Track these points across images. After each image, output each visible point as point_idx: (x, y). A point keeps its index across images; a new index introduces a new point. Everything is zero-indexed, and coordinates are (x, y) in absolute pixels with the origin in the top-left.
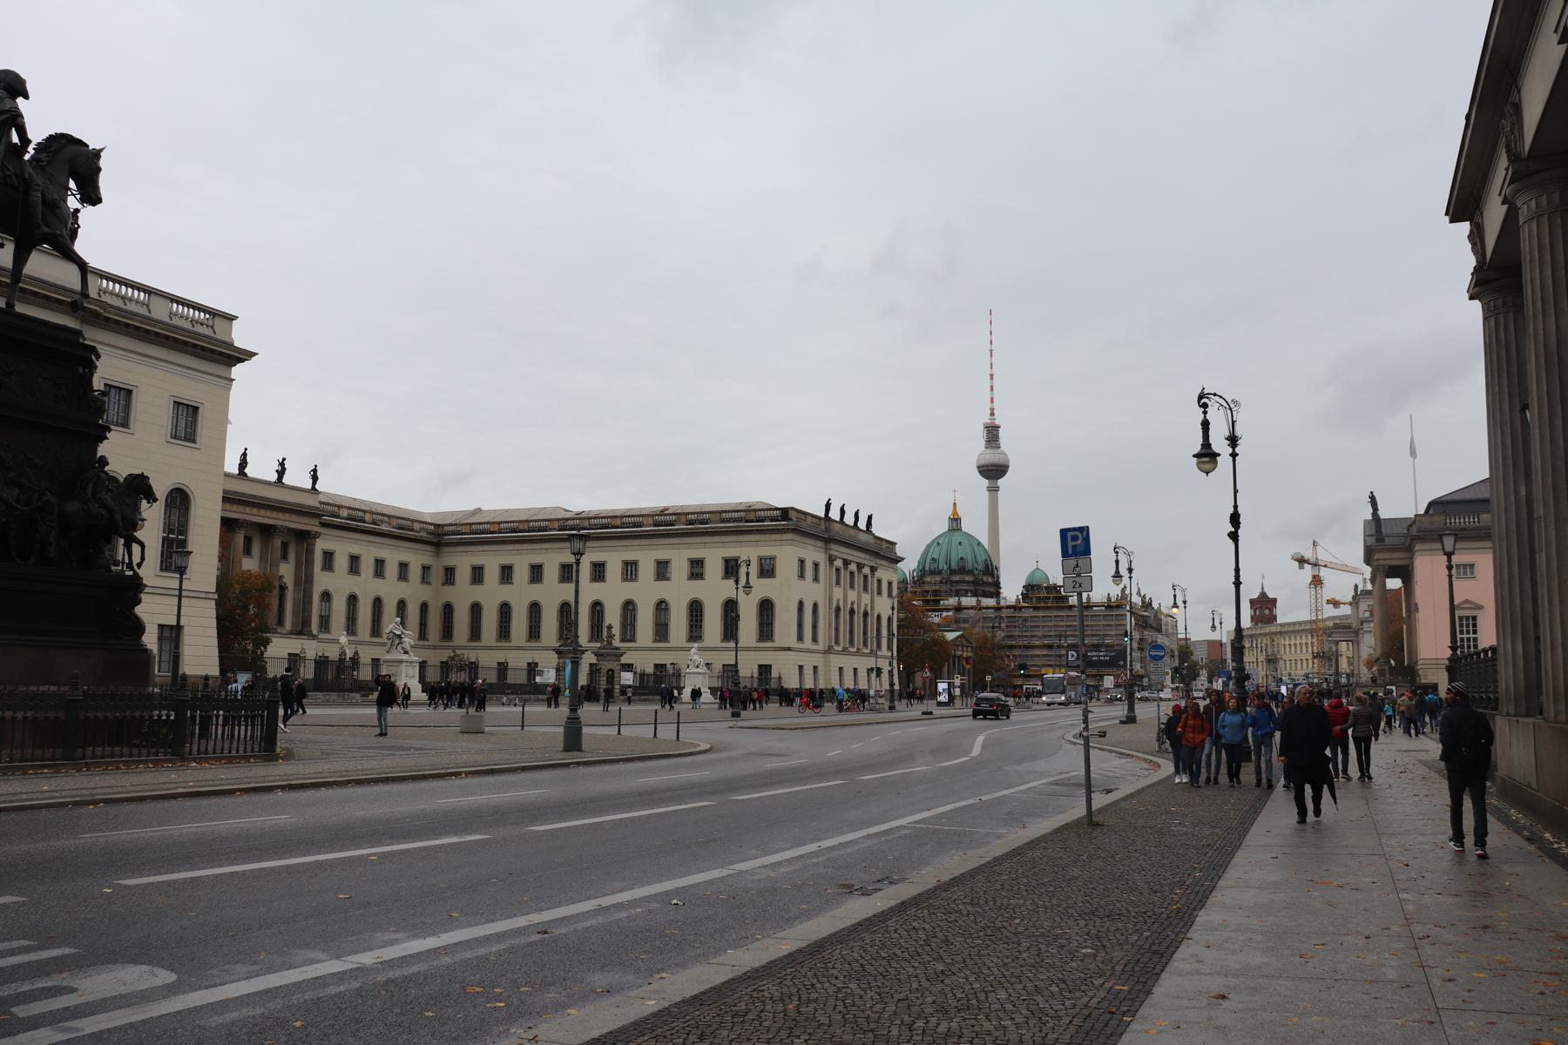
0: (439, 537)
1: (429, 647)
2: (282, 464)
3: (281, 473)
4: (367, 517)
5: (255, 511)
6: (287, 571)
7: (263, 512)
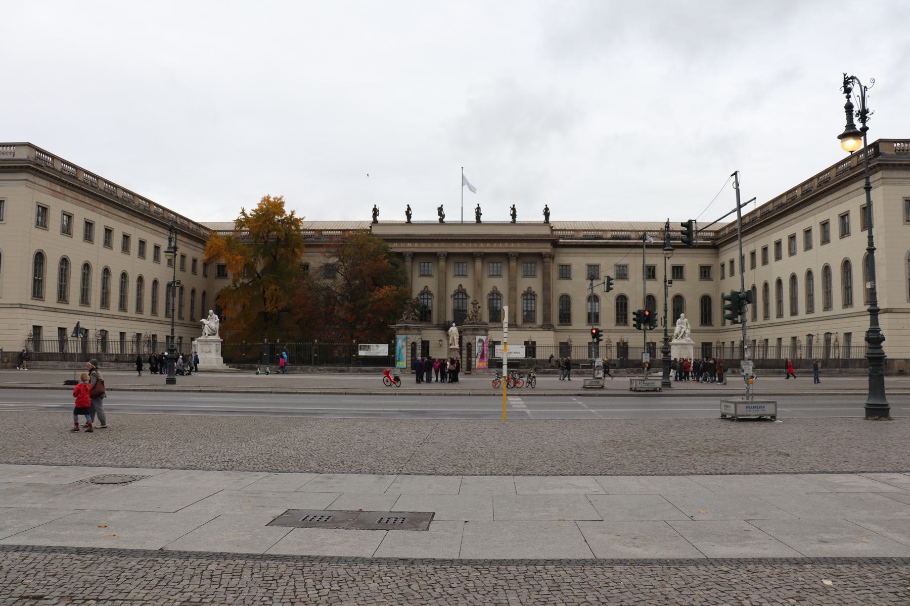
0: (718, 240)
1: (714, 331)
2: (513, 209)
3: (514, 215)
4: (633, 235)
5: (488, 245)
6: (535, 284)
7: (495, 245)
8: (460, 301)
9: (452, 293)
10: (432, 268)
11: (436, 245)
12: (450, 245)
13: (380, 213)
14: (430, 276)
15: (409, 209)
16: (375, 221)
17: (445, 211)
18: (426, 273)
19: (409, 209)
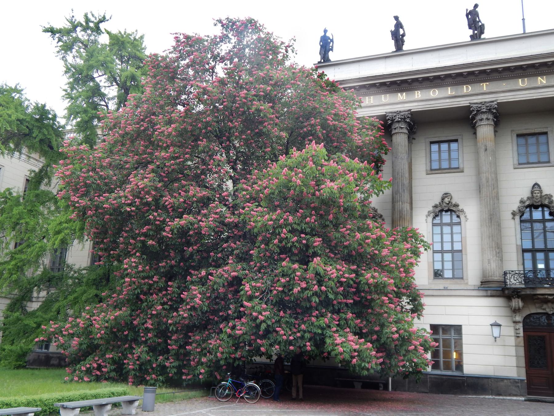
8: (538, 226)
9: (515, 206)
10: (462, 153)
11: (466, 89)
12: (504, 85)
13: (336, 45)
14: (458, 170)
15: (399, 25)
16: (325, 61)
17: (483, 18)
18: (445, 165)
19: (399, 25)
